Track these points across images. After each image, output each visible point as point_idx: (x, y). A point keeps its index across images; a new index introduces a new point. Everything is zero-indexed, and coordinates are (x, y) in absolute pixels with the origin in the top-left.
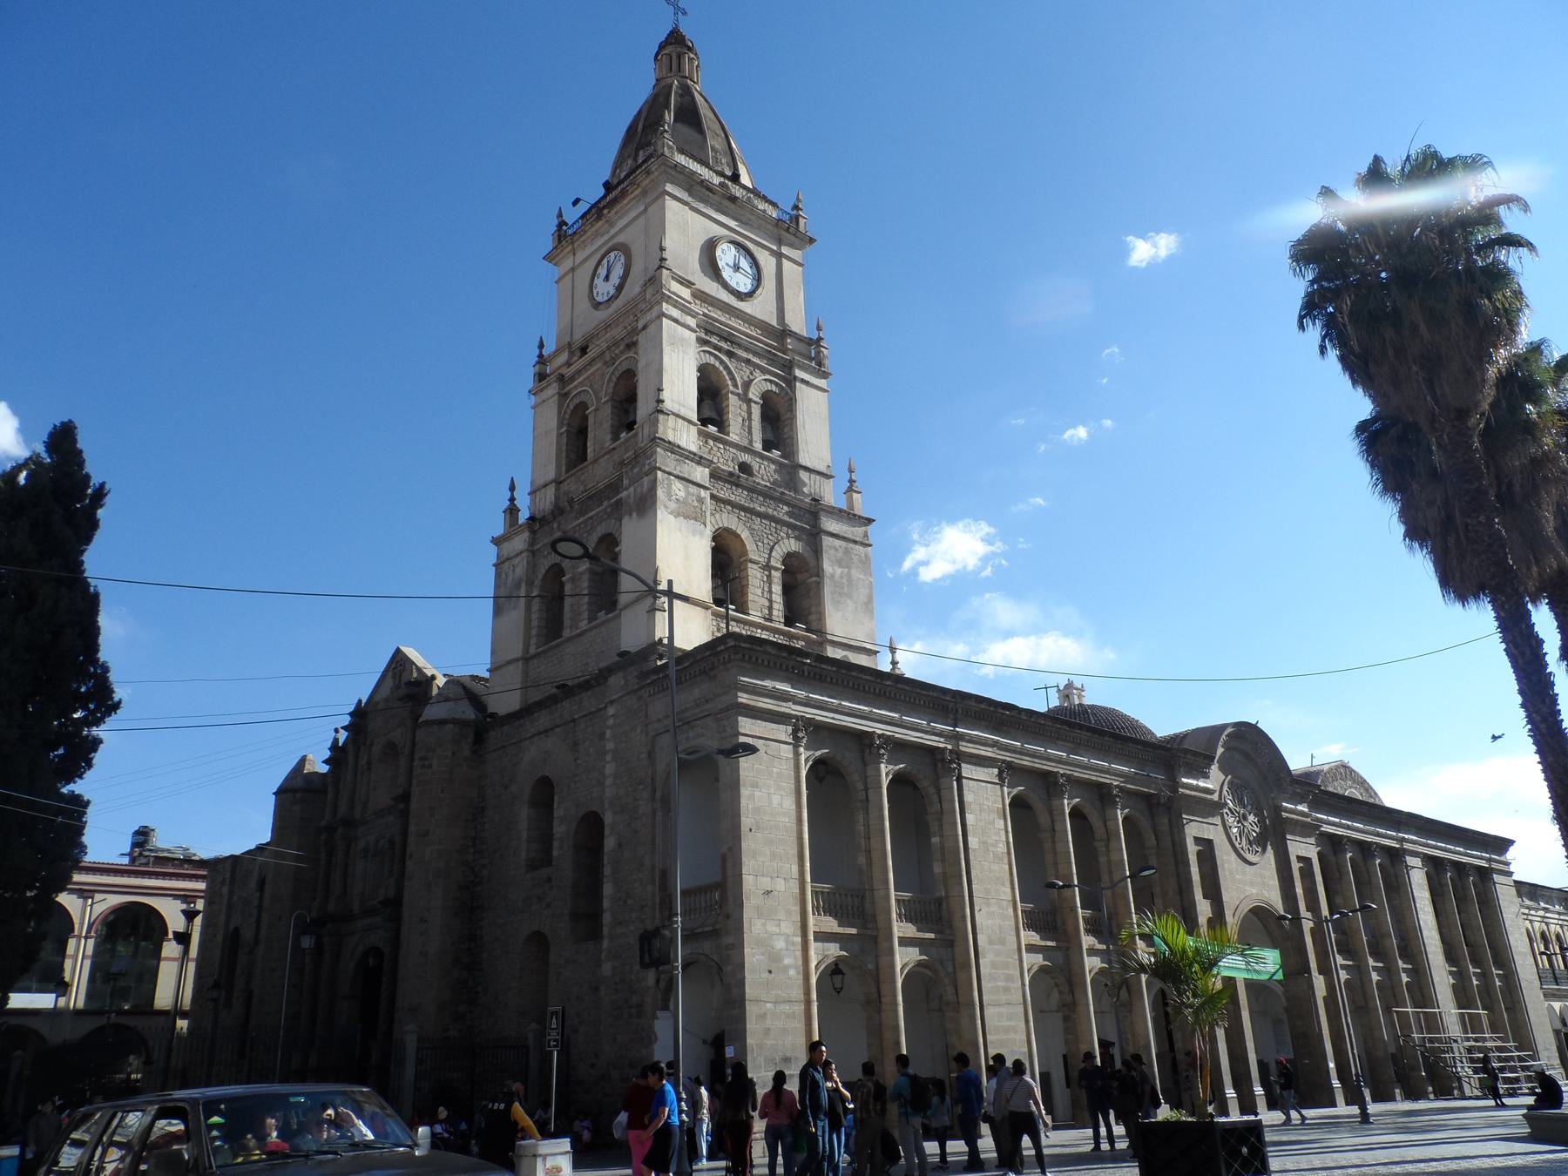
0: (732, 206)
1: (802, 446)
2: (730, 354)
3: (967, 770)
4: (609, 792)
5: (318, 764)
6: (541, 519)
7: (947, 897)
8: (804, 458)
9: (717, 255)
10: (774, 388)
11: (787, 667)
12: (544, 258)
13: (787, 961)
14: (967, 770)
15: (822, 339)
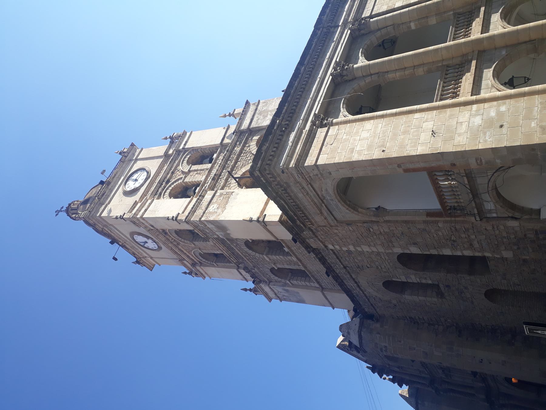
0: (112, 184)
1: (212, 143)
2: (168, 181)
3: (366, 13)
4: (381, 250)
5: (405, 390)
6: (253, 278)
7: (454, 10)
8: (218, 142)
9: (129, 190)
10: (187, 159)
11: (280, 135)
12: (151, 271)
13: (493, 113)
14: (366, 13)
15: (170, 136)
